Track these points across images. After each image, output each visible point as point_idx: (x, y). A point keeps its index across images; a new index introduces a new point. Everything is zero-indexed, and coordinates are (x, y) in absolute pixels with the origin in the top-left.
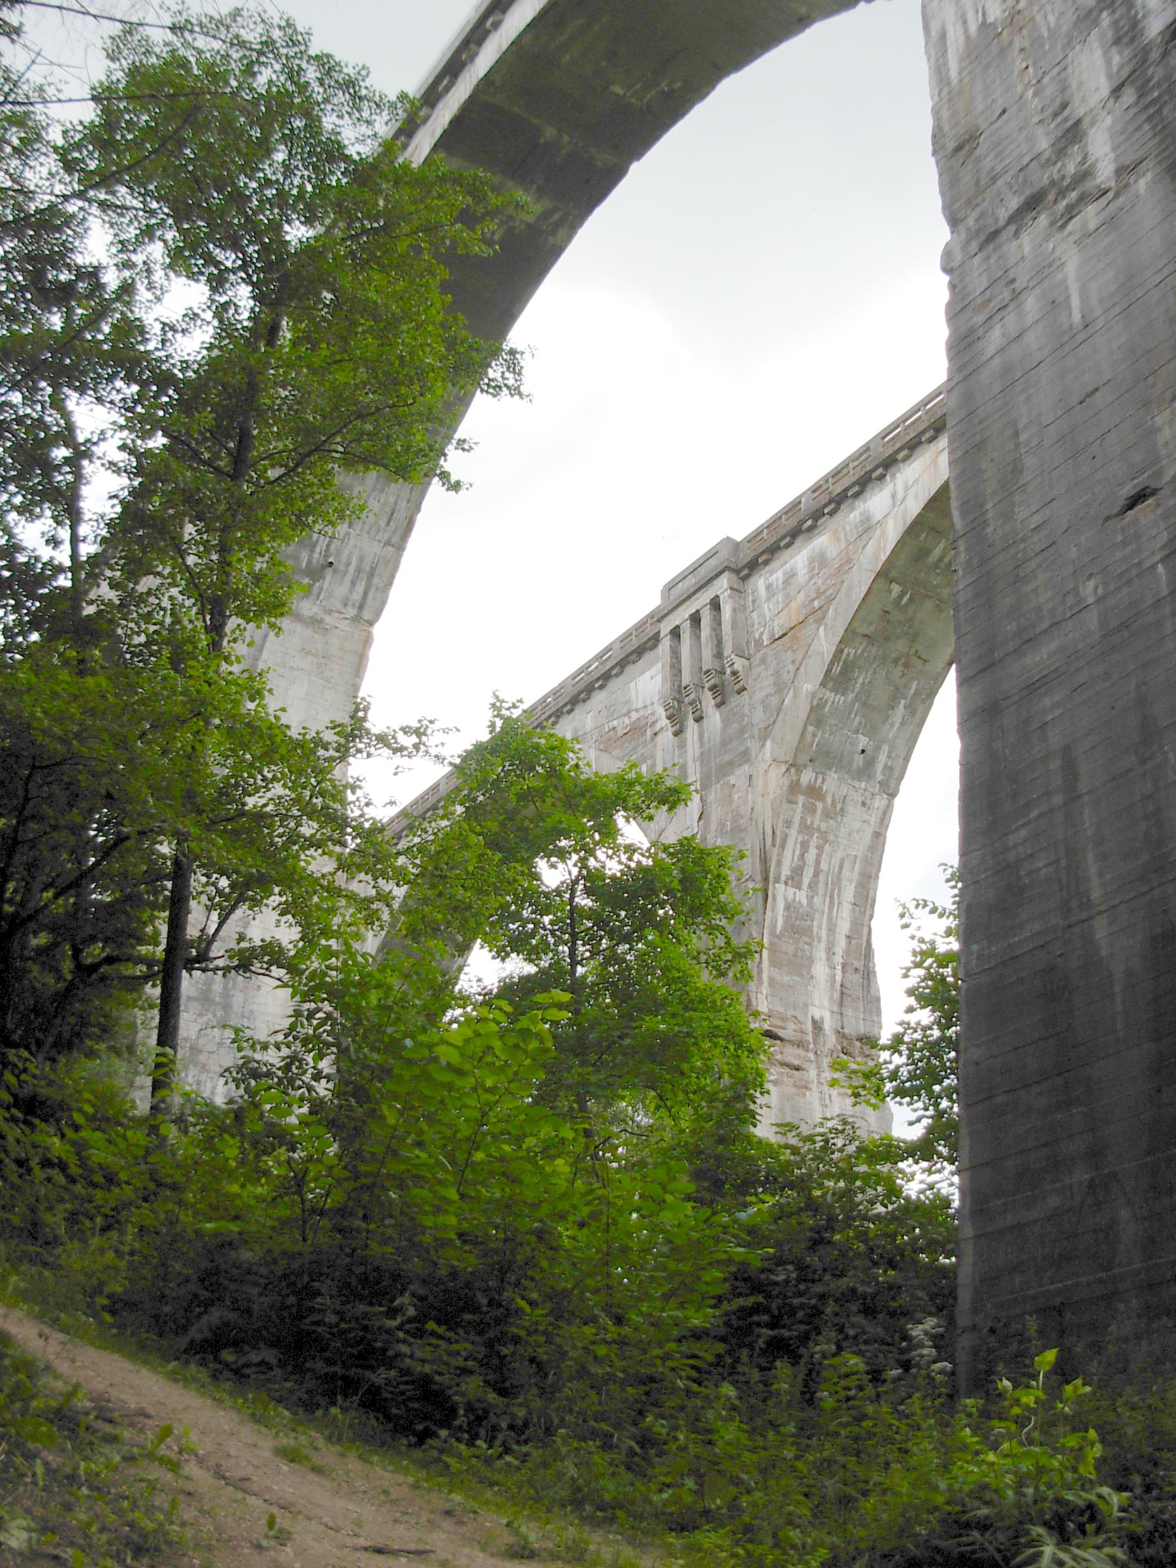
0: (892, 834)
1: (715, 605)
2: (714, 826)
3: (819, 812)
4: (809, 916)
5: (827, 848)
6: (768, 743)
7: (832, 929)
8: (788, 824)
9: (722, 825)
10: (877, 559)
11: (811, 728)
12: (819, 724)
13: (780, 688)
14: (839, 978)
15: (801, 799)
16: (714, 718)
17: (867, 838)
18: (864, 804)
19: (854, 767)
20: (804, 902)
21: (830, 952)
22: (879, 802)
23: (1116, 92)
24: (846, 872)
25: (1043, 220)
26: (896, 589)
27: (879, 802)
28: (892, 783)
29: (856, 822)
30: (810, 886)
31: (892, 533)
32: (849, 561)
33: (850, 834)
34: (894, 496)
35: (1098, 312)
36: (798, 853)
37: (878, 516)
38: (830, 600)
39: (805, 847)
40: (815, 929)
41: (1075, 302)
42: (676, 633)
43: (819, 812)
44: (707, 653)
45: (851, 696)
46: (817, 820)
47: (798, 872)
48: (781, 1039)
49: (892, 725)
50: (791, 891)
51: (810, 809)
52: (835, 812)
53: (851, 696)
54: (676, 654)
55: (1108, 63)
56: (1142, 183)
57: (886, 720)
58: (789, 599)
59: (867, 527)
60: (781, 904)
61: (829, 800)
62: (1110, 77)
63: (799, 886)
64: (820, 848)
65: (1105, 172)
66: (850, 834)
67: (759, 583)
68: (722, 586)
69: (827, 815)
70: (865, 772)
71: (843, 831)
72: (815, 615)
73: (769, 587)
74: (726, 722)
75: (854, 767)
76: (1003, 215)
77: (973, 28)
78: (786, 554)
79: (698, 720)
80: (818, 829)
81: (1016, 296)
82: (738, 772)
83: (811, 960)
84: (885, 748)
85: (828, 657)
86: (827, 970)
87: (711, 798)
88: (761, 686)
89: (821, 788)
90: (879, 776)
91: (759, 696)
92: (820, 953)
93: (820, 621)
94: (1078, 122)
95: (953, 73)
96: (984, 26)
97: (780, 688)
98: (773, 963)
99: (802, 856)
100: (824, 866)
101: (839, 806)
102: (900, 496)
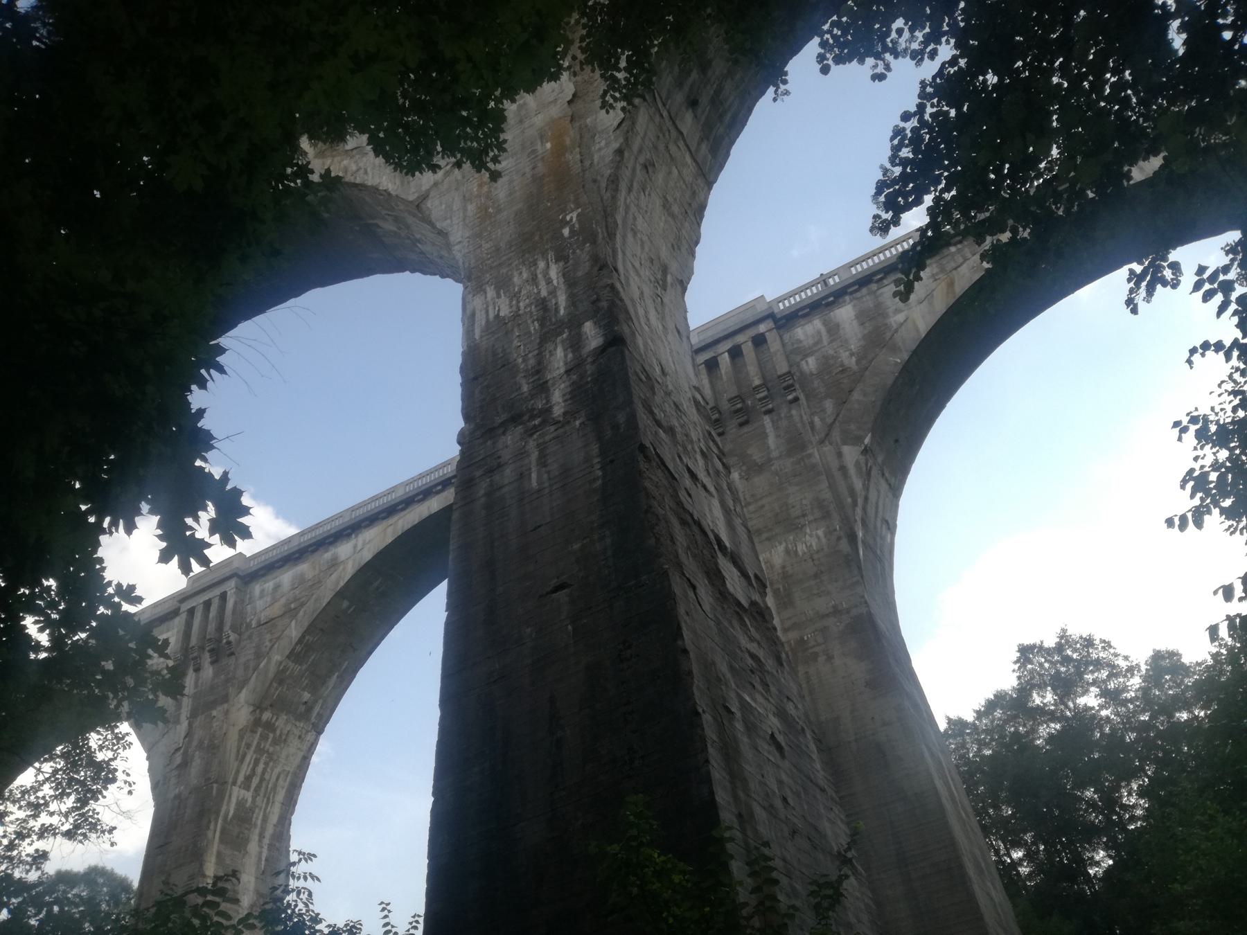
0: (315, 759)
1: (223, 597)
2: (195, 743)
4: (252, 810)
6: (244, 691)
7: (265, 819)
8: (248, 746)
9: (201, 742)
10: (338, 583)
11: (275, 685)
12: (281, 682)
13: (259, 656)
15: (260, 730)
16: (208, 671)
17: (298, 760)
18: (300, 737)
20: (250, 800)
21: (261, 836)
22: (310, 737)
23: (568, 372)
24: (281, 782)
25: (520, 429)
29: (293, 749)
31: (350, 570)
32: (320, 582)
33: (287, 756)
34: (355, 547)
35: (546, 485)
37: (342, 557)
38: (302, 605)
41: (534, 476)
42: (191, 612)
44: (212, 627)
45: (304, 667)
46: (267, 745)
47: (248, 779)
50: (243, 792)
51: (264, 738)
52: (281, 741)
53: (304, 667)
54: (189, 625)
55: (566, 356)
56: (577, 423)
58: (274, 601)
59: (334, 564)
60: (234, 800)
62: (566, 364)
63: (247, 788)
64: (266, 764)
65: (558, 411)
66: (287, 756)
67: (257, 588)
68: (230, 587)
71: (284, 753)
72: (290, 612)
73: (262, 591)
74: (216, 675)
76: (498, 420)
77: (491, 316)
78: (279, 571)
79: (197, 670)
81: (500, 466)
82: (219, 708)
83: (247, 840)
84: (320, 701)
85: (295, 640)
87: (196, 724)
88: (246, 654)
90: (313, 720)
91: (242, 660)
92: (255, 837)
93: (294, 617)
94: (547, 382)
95: (477, 337)
96: (497, 316)
97: (259, 656)
98: (222, 841)
99: (253, 770)
100: (267, 777)
102: (359, 548)
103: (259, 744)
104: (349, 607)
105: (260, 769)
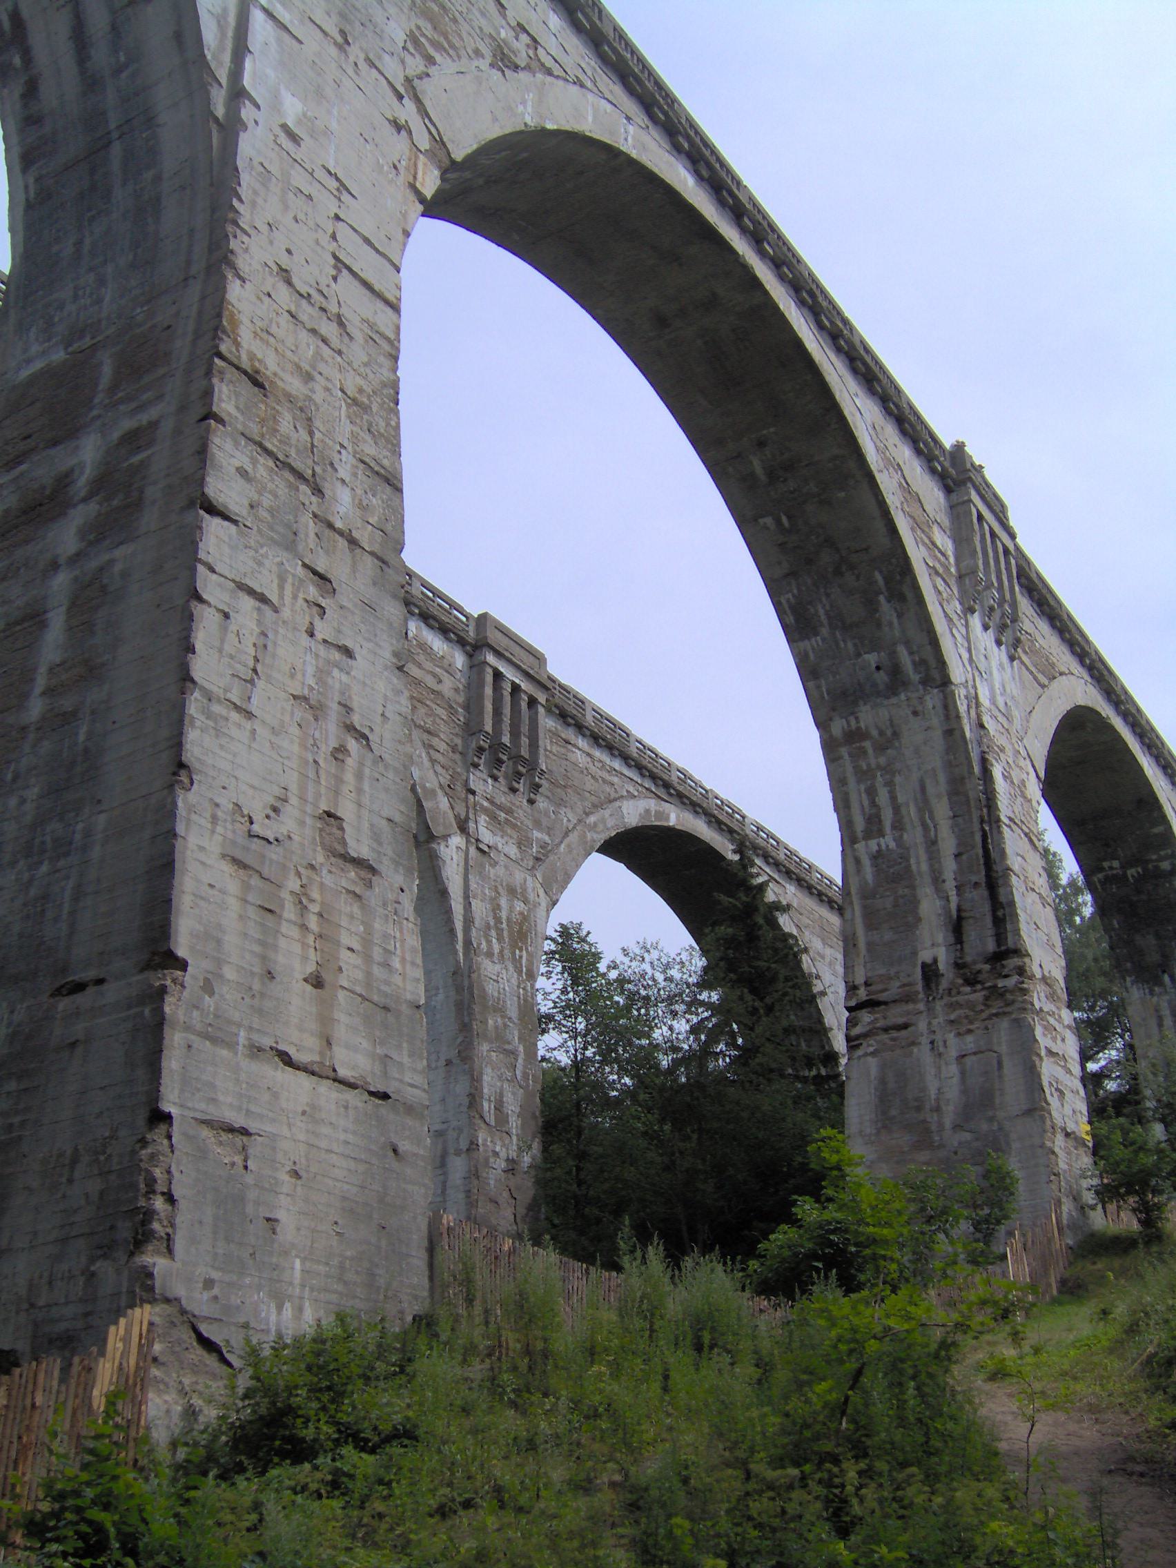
3: (870, 751)
4: (905, 858)
5: (898, 779)
14: (953, 906)
18: (915, 713)
19: (882, 687)
20: (892, 845)
24: (931, 790)
26: (769, 521)
27: (932, 700)
28: (936, 675)
30: (894, 827)
36: (866, 803)
39: (871, 792)
40: (914, 867)
43: (870, 751)
45: (825, 631)
48: (885, 1003)
49: (891, 624)
50: (873, 845)
52: (889, 739)
53: (825, 631)
57: (879, 625)
61: (875, 733)
64: (890, 784)
69: (881, 749)
70: (897, 681)
75: (882, 687)
80: (879, 767)
83: (914, 903)
84: (902, 651)
86: (938, 903)
89: (859, 728)
90: (915, 677)
99: (873, 803)
101: (889, 733)
103: (857, 769)
104: (778, 522)
105: (883, 797)
